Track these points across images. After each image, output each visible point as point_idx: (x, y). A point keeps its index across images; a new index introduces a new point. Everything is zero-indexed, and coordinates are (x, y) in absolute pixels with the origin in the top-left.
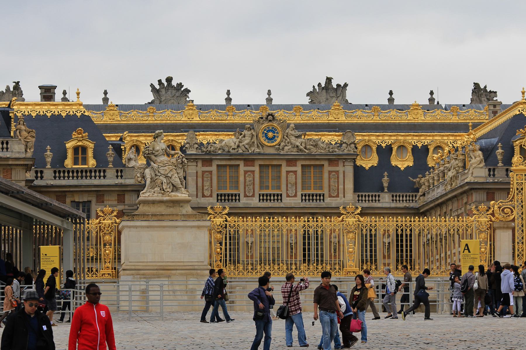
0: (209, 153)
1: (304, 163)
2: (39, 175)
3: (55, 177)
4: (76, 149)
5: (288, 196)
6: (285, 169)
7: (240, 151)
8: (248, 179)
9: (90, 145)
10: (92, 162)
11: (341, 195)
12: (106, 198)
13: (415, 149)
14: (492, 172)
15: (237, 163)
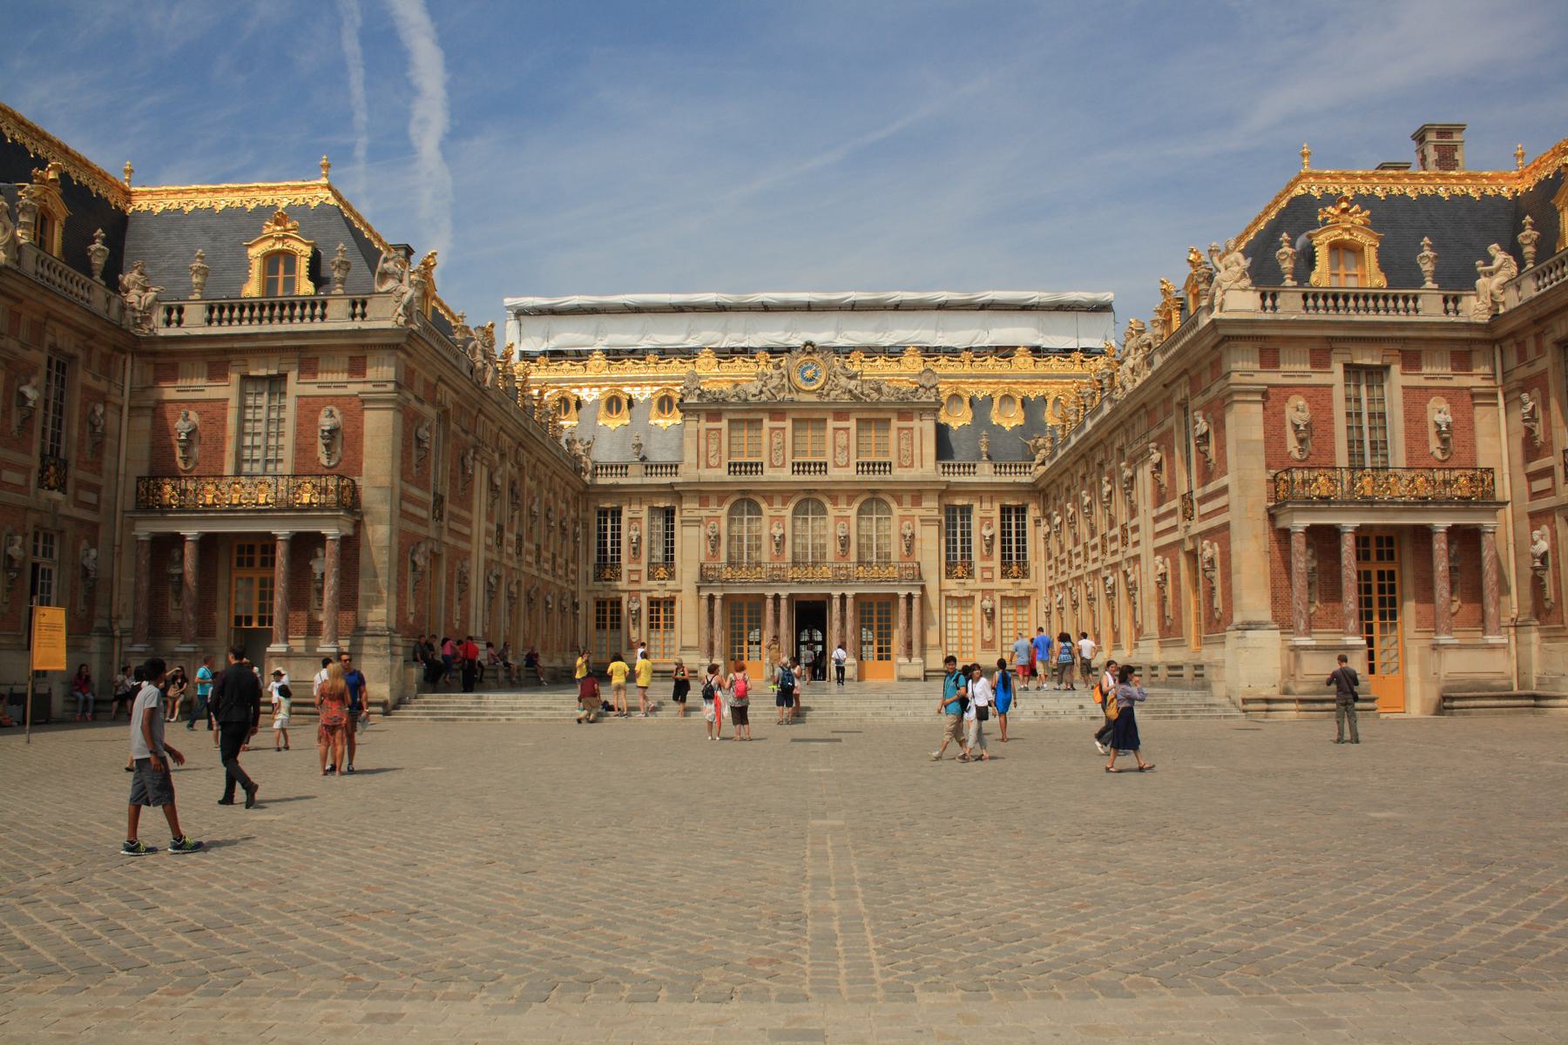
0: (716, 401)
1: (861, 416)
2: (175, 316)
3: (210, 321)
4: (271, 259)
5: (836, 465)
6: (831, 424)
7: (764, 398)
8: (775, 441)
9: (303, 250)
10: (305, 287)
11: (917, 464)
12: (321, 365)
13: (1025, 402)
14: (1269, 296)
15: (759, 416)
